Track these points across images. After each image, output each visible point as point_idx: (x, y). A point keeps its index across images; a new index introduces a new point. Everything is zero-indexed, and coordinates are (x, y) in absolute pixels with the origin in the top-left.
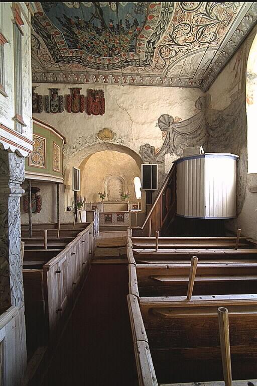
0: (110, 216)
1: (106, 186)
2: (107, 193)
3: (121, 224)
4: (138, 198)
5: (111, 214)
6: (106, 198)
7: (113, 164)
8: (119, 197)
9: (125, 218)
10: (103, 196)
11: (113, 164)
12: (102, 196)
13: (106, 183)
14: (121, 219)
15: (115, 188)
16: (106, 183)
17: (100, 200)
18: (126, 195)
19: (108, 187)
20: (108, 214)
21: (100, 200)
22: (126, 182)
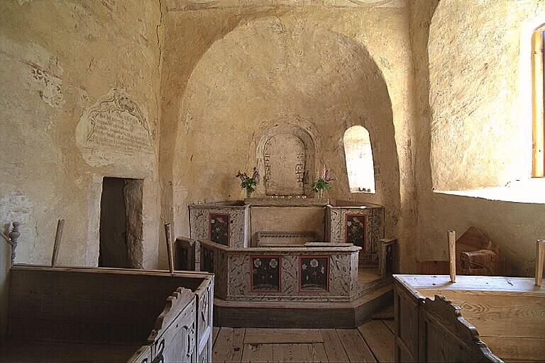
0: (273, 264)
1: (260, 156)
2: (262, 173)
3: (315, 301)
4: (353, 191)
5: (278, 257)
6: (260, 189)
7: (282, 87)
8: (297, 185)
9: (334, 272)
10: (252, 181)
11: (282, 87)
12: (249, 184)
13: (261, 145)
14: (316, 274)
15: (286, 162)
16: (261, 145)
17: (243, 194)
18: (321, 181)
19: (266, 156)
20: (265, 257)
21: (243, 194)
22: (317, 143)
